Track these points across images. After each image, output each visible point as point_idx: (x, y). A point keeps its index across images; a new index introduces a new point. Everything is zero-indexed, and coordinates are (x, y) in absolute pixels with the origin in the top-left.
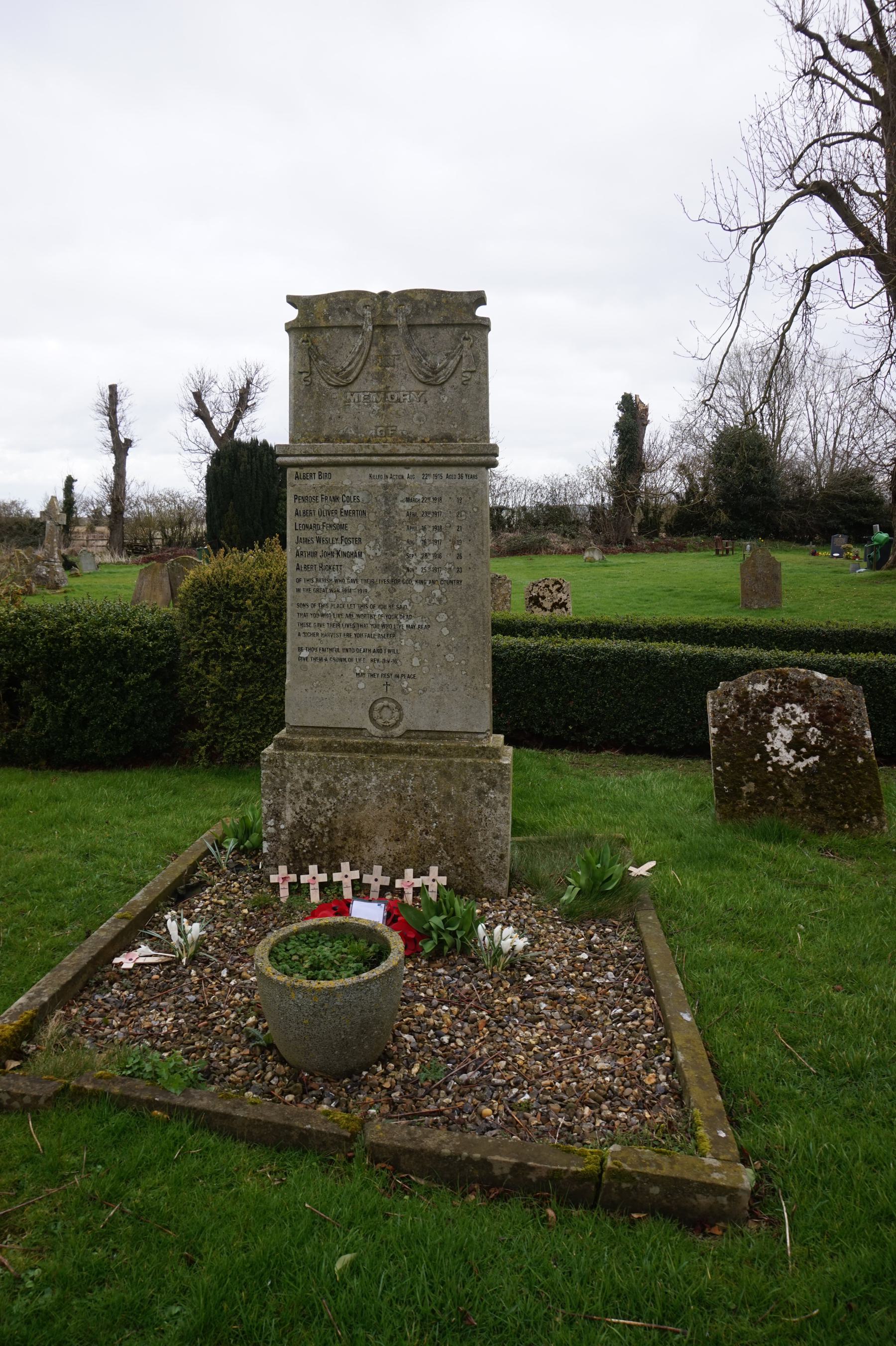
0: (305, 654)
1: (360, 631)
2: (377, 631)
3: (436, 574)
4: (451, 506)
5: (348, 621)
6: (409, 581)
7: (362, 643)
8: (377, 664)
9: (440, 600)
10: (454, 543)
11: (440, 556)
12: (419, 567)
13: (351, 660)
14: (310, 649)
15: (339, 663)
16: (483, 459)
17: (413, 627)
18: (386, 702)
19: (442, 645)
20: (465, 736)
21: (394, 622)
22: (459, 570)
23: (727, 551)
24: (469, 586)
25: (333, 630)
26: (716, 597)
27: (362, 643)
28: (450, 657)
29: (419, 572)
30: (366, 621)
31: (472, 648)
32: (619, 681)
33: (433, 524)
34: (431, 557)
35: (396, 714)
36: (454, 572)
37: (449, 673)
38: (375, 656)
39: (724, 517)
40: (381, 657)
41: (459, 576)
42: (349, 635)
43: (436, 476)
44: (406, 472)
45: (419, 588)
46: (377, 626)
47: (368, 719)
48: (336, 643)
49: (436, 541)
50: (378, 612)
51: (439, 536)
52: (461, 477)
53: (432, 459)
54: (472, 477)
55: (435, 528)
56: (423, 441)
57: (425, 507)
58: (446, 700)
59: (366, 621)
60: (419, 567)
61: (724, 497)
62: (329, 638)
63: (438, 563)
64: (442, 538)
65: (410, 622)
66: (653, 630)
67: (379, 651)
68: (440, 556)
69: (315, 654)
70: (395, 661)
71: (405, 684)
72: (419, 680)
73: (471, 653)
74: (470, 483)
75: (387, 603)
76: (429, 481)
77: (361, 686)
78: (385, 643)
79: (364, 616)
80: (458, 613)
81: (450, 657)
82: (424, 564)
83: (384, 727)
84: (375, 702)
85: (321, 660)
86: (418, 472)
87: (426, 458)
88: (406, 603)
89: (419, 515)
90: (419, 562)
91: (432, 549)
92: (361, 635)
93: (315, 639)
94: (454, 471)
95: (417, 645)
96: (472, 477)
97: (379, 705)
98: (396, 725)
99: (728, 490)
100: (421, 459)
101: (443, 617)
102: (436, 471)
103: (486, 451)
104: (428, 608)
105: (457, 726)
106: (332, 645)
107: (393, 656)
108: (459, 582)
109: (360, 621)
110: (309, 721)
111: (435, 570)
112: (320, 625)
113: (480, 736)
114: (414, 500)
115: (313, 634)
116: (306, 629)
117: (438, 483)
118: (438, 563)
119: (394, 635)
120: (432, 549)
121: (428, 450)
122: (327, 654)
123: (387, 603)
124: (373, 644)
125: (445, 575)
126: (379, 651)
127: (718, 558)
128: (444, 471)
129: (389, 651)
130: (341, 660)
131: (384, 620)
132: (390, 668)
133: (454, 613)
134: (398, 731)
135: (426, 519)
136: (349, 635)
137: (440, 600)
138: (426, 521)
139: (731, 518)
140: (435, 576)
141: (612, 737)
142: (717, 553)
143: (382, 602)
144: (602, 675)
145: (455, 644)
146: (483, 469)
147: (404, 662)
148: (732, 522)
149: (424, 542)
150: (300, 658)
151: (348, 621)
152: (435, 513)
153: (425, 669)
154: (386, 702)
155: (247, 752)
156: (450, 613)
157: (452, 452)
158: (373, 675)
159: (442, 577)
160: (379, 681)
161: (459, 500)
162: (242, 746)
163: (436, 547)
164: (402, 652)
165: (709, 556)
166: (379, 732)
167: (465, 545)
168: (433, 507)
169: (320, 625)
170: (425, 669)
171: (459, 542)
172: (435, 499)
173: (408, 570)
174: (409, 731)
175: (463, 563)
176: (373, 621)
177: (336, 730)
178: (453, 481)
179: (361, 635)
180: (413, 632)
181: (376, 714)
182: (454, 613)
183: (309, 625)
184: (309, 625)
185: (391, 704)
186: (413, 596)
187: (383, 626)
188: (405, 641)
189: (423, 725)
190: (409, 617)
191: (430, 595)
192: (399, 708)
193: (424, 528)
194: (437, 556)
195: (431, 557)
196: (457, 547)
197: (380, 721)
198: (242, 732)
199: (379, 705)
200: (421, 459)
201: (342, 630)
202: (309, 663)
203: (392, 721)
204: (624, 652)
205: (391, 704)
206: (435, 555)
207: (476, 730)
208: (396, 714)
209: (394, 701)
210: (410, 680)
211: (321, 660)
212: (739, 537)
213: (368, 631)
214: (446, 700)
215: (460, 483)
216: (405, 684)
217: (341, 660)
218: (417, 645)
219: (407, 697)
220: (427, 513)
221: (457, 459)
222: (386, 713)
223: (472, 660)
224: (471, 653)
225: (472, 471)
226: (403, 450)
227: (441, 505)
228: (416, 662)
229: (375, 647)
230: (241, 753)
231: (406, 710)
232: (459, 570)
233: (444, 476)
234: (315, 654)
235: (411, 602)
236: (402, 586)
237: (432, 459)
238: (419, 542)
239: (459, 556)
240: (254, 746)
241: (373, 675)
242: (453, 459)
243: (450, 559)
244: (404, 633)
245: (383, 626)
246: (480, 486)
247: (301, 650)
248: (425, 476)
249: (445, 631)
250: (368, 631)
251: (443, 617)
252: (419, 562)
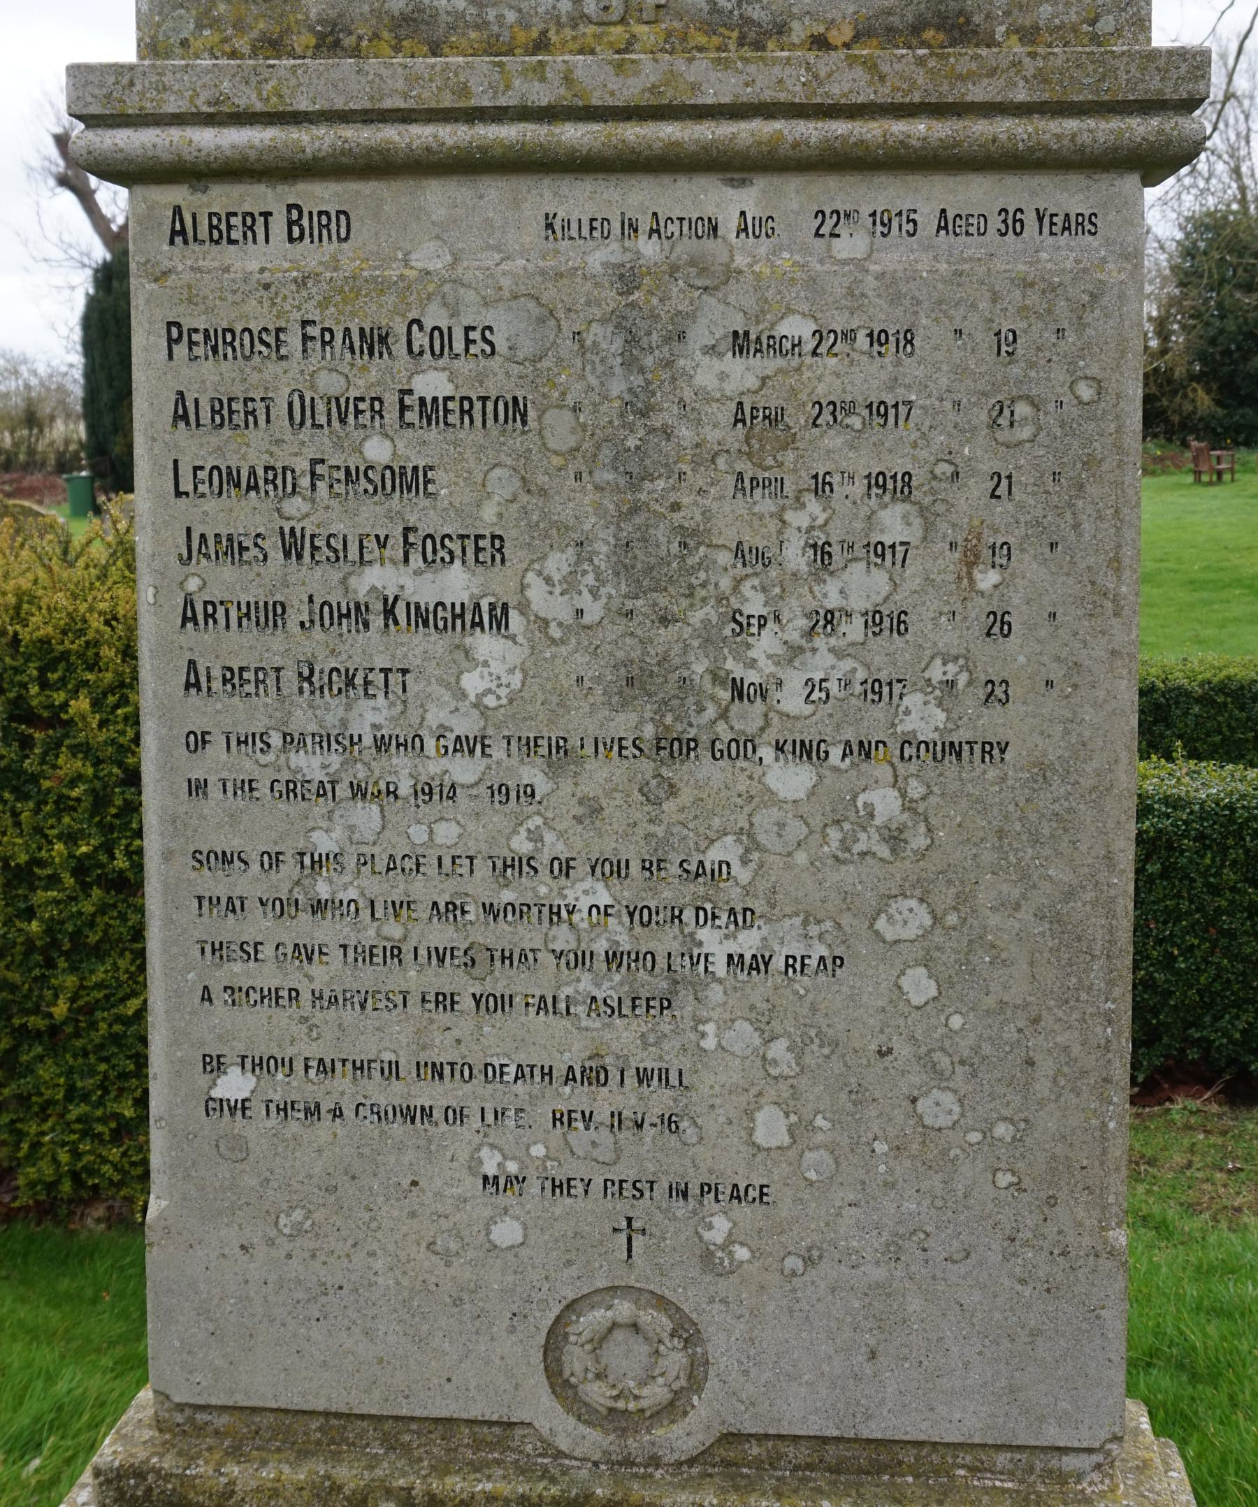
0: (235, 1085)
1: (501, 981)
2: (586, 983)
3: (878, 713)
4: (960, 370)
5: (441, 935)
6: (744, 747)
7: (498, 1039)
8: (580, 1136)
9: (895, 838)
10: (971, 561)
11: (900, 624)
12: (795, 681)
13: (457, 1115)
14: (258, 1065)
15: (398, 1128)
16: (1140, 128)
17: (760, 963)
18: (624, 1309)
19: (903, 1050)
20: (1002, 1459)
21: (665, 941)
22: (995, 692)
23: (1220, 474)
24: (1042, 771)
25: (367, 977)
26: (1239, 583)
27: (498, 1039)
28: (939, 1107)
29: (792, 700)
30: (527, 935)
31: (1046, 1066)
32: (1215, 891)
33: (865, 463)
34: (854, 630)
35: (675, 1361)
36: (970, 701)
37: (935, 1182)
38: (576, 1097)
39: (1203, 400)
40: (604, 1101)
41: (993, 723)
42: (446, 1001)
43: (882, 222)
44: (728, 202)
45: (790, 780)
46: (581, 959)
47: (545, 1398)
48: (393, 1037)
49: (880, 550)
50: (589, 893)
51: (895, 523)
52: (1013, 223)
53: (870, 130)
54: (1076, 225)
55: (878, 482)
56: (820, 43)
57: (828, 377)
58: (915, 1304)
59: (527, 935)
60: (795, 681)
61: (1203, 357)
62: (349, 1015)
63: (887, 655)
64: (913, 534)
65: (748, 942)
66: (1188, 694)
67: (593, 1074)
68: (900, 624)
69: (280, 1087)
70: (670, 1123)
71: (719, 1229)
72: (785, 1210)
73: (1042, 1087)
74: (1060, 254)
75: (633, 853)
76: (851, 245)
77: (507, 1232)
78: (623, 1038)
79: (521, 911)
80: (984, 898)
81: (939, 1107)
82: (821, 663)
83: (616, 1419)
84: (571, 1306)
85: (313, 1111)
86: (795, 198)
87: (840, 127)
88: (724, 850)
89: (797, 419)
90: (794, 652)
91: (860, 586)
92: (503, 1003)
93: (284, 1018)
94: (977, 193)
95: (778, 1049)
96: (1076, 225)
97: (596, 1318)
98: (673, 1408)
99: (1213, 342)
100: (811, 131)
101: (908, 920)
102: (887, 193)
103: (1153, 85)
104: (835, 876)
105: (961, 1420)
106: (365, 1048)
107: (660, 1100)
108: (992, 750)
109: (502, 934)
110: (264, 1383)
111: (875, 689)
112: (305, 953)
113: (1070, 1463)
114: (775, 346)
115: (274, 996)
116: (239, 972)
117: (895, 255)
118: (887, 655)
119: (666, 1004)
120: (860, 586)
121: (847, 83)
122: (343, 1087)
123: (633, 853)
124: (563, 1043)
125: (922, 717)
126: (593, 1074)
127: (1200, 490)
128: (928, 196)
129: (643, 1077)
130: (409, 1115)
131: (619, 933)
132: (644, 1155)
133: (962, 900)
134: (682, 1437)
135: (834, 440)
136: (446, 1001)
137: (895, 838)
138: (830, 449)
139: (1218, 403)
140: (873, 722)
141: (1193, 1054)
142: (1198, 481)
143: (606, 847)
144: (1164, 875)
145: (964, 1046)
146: (1133, 179)
147: (712, 1126)
148: (1220, 412)
149: (822, 552)
150: (214, 1106)
151: (441, 935)
152: (880, 411)
153: (816, 1163)
154: (624, 1309)
155: (92, 1172)
156: (944, 896)
157: (978, 93)
158: (561, 1187)
159: (909, 725)
160: (592, 1213)
161: (1005, 344)
162: (76, 1154)
163: (880, 580)
164: (707, 1083)
165: (1179, 486)
166: (593, 1441)
167: (1027, 565)
168: (867, 377)
169: (305, 953)
170: (816, 1163)
171: (1002, 553)
172: (878, 338)
173: (738, 690)
174: (731, 1438)
175: (1015, 656)
176: (563, 938)
177: (393, 1430)
178: (971, 247)
179: (503, 1003)
180: (759, 988)
181: (576, 1360)
182: (962, 900)
183: (250, 951)
184: (250, 951)
185: (648, 1317)
186: (765, 820)
187: (613, 958)
188: (721, 1032)
189: (802, 1412)
190: (742, 917)
191: (846, 814)
192: (688, 1333)
193: (821, 486)
194: (888, 621)
195: (854, 630)
196: (988, 579)
197: (598, 1394)
198: (75, 1111)
199: (596, 1318)
200: (811, 131)
201: (414, 978)
202: (258, 1130)
203: (655, 1394)
204: (1232, 808)
205: (648, 1317)
206: (874, 619)
207: (1053, 1435)
208: (675, 1361)
209: (661, 1302)
210: (743, 1212)
211: (313, 1111)
212: (1237, 444)
213: (542, 979)
214: (915, 1304)
215: (1010, 257)
216: (719, 1229)
217: (409, 1115)
218: (778, 1049)
219: (723, 1287)
220: (838, 410)
221: (1003, 128)
222: (626, 1357)
223: (1048, 1122)
224: (1042, 1087)
225: (1068, 195)
226: (719, 87)
227: (912, 369)
228: (771, 1127)
229: (575, 1055)
230: (75, 1177)
231: (722, 1347)
232: (995, 692)
233: (927, 221)
234: (280, 1087)
235: (747, 835)
236: (706, 771)
237: (870, 130)
238: (796, 557)
239: (999, 624)
240: (114, 1153)
241: (561, 1187)
242: (980, 129)
243: (949, 638)
244: (715, 993)
245: (613, 958)
246: (1114, 273)
247: (214, 1065)
248: (829, 223)
249: (920, 986)
250: (542, 979)
251: (908, 920)
252: (794, 652)
